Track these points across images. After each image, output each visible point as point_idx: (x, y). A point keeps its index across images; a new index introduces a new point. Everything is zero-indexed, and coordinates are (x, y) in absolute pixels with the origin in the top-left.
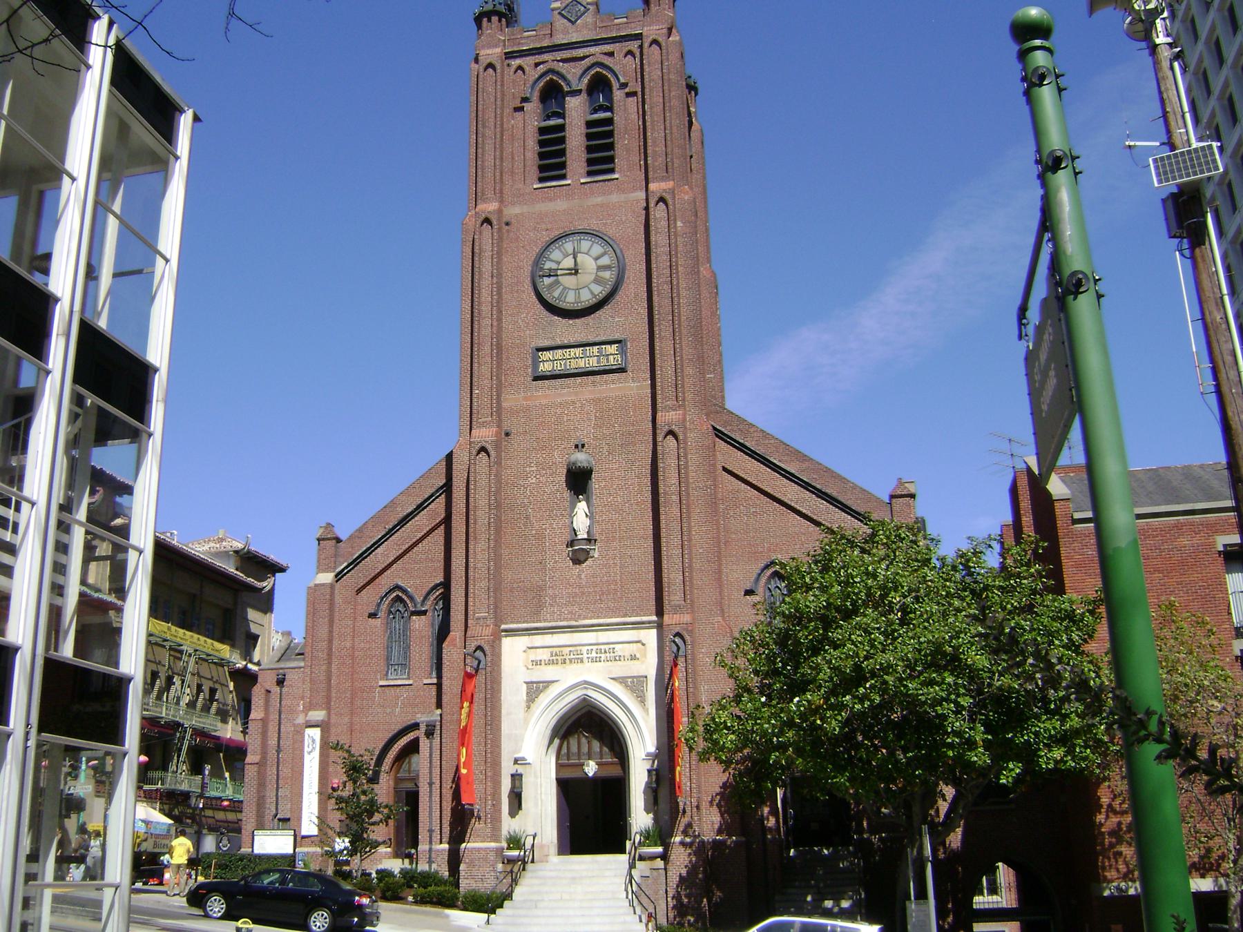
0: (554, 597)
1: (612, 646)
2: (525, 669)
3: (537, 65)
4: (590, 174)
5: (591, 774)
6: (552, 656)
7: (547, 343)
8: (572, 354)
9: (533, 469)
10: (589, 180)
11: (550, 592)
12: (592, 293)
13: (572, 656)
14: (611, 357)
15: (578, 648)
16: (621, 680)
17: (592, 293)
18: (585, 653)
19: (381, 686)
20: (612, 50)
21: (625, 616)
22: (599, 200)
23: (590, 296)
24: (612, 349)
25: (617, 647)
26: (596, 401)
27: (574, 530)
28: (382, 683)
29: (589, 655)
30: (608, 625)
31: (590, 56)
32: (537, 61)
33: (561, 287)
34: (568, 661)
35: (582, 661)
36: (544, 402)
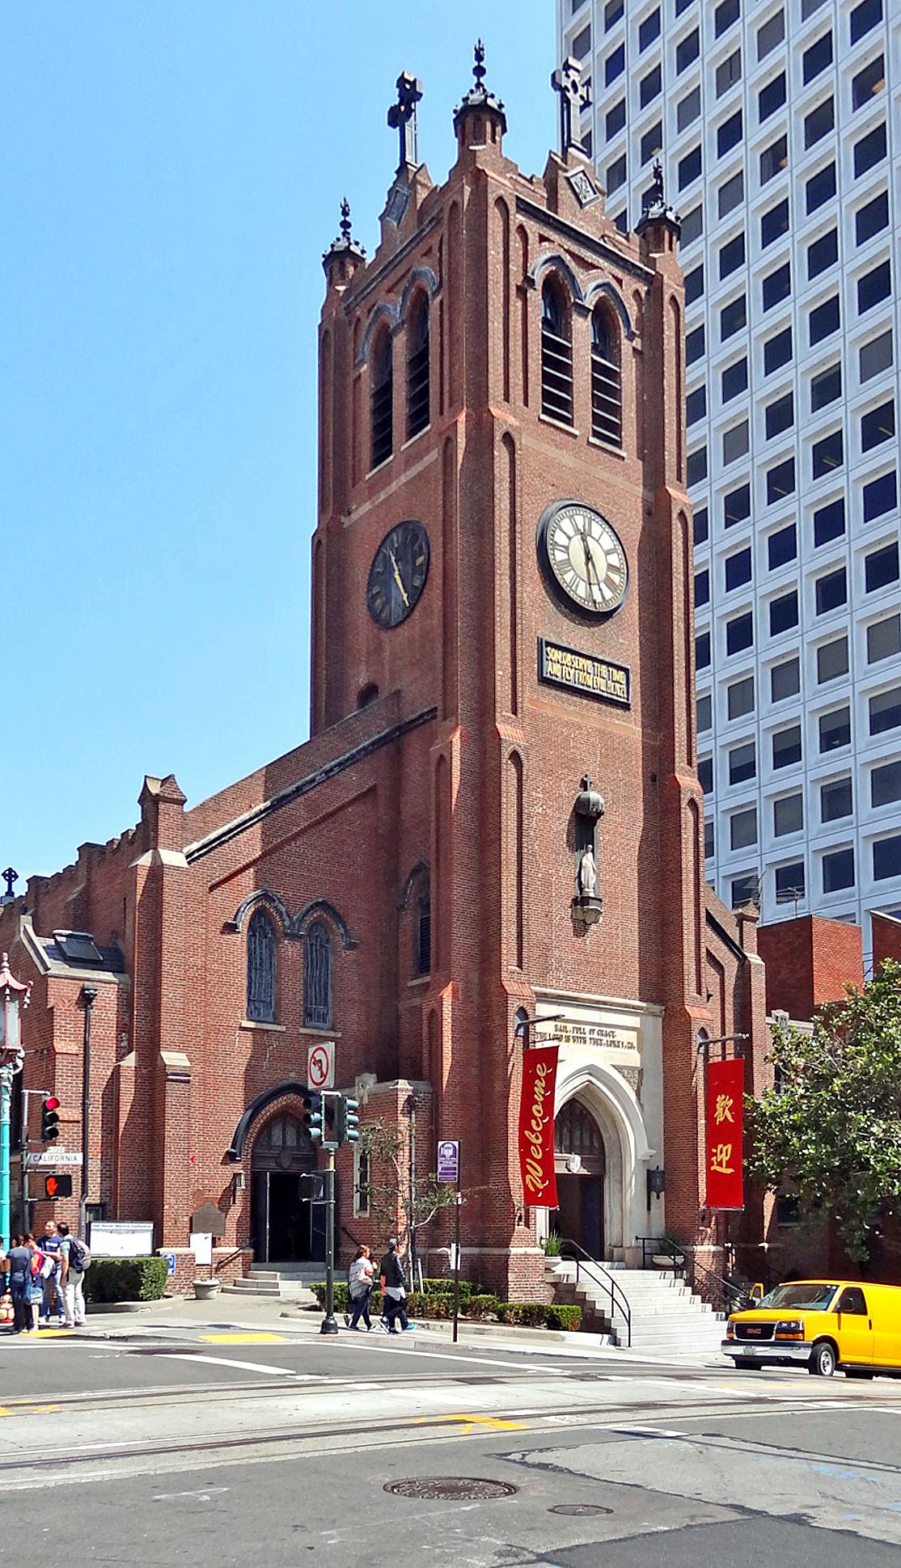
0: (560, 960)
1: (613, 1030)
4: (596, 434)
7: (553, 640)
11: (556, 952)
13: (575, 1034)
14: (618, 685)
15: (582, 1026)
18: (588, 1032)
20: (620, 274)
22: (605, 475)
24: (620, 676)
25: (618, 1032)
26: (602, 733)
27: (580, 883)
29: (591, 1036)
30: (612, 1004)
31: (598, 268)
33: (572, 572)
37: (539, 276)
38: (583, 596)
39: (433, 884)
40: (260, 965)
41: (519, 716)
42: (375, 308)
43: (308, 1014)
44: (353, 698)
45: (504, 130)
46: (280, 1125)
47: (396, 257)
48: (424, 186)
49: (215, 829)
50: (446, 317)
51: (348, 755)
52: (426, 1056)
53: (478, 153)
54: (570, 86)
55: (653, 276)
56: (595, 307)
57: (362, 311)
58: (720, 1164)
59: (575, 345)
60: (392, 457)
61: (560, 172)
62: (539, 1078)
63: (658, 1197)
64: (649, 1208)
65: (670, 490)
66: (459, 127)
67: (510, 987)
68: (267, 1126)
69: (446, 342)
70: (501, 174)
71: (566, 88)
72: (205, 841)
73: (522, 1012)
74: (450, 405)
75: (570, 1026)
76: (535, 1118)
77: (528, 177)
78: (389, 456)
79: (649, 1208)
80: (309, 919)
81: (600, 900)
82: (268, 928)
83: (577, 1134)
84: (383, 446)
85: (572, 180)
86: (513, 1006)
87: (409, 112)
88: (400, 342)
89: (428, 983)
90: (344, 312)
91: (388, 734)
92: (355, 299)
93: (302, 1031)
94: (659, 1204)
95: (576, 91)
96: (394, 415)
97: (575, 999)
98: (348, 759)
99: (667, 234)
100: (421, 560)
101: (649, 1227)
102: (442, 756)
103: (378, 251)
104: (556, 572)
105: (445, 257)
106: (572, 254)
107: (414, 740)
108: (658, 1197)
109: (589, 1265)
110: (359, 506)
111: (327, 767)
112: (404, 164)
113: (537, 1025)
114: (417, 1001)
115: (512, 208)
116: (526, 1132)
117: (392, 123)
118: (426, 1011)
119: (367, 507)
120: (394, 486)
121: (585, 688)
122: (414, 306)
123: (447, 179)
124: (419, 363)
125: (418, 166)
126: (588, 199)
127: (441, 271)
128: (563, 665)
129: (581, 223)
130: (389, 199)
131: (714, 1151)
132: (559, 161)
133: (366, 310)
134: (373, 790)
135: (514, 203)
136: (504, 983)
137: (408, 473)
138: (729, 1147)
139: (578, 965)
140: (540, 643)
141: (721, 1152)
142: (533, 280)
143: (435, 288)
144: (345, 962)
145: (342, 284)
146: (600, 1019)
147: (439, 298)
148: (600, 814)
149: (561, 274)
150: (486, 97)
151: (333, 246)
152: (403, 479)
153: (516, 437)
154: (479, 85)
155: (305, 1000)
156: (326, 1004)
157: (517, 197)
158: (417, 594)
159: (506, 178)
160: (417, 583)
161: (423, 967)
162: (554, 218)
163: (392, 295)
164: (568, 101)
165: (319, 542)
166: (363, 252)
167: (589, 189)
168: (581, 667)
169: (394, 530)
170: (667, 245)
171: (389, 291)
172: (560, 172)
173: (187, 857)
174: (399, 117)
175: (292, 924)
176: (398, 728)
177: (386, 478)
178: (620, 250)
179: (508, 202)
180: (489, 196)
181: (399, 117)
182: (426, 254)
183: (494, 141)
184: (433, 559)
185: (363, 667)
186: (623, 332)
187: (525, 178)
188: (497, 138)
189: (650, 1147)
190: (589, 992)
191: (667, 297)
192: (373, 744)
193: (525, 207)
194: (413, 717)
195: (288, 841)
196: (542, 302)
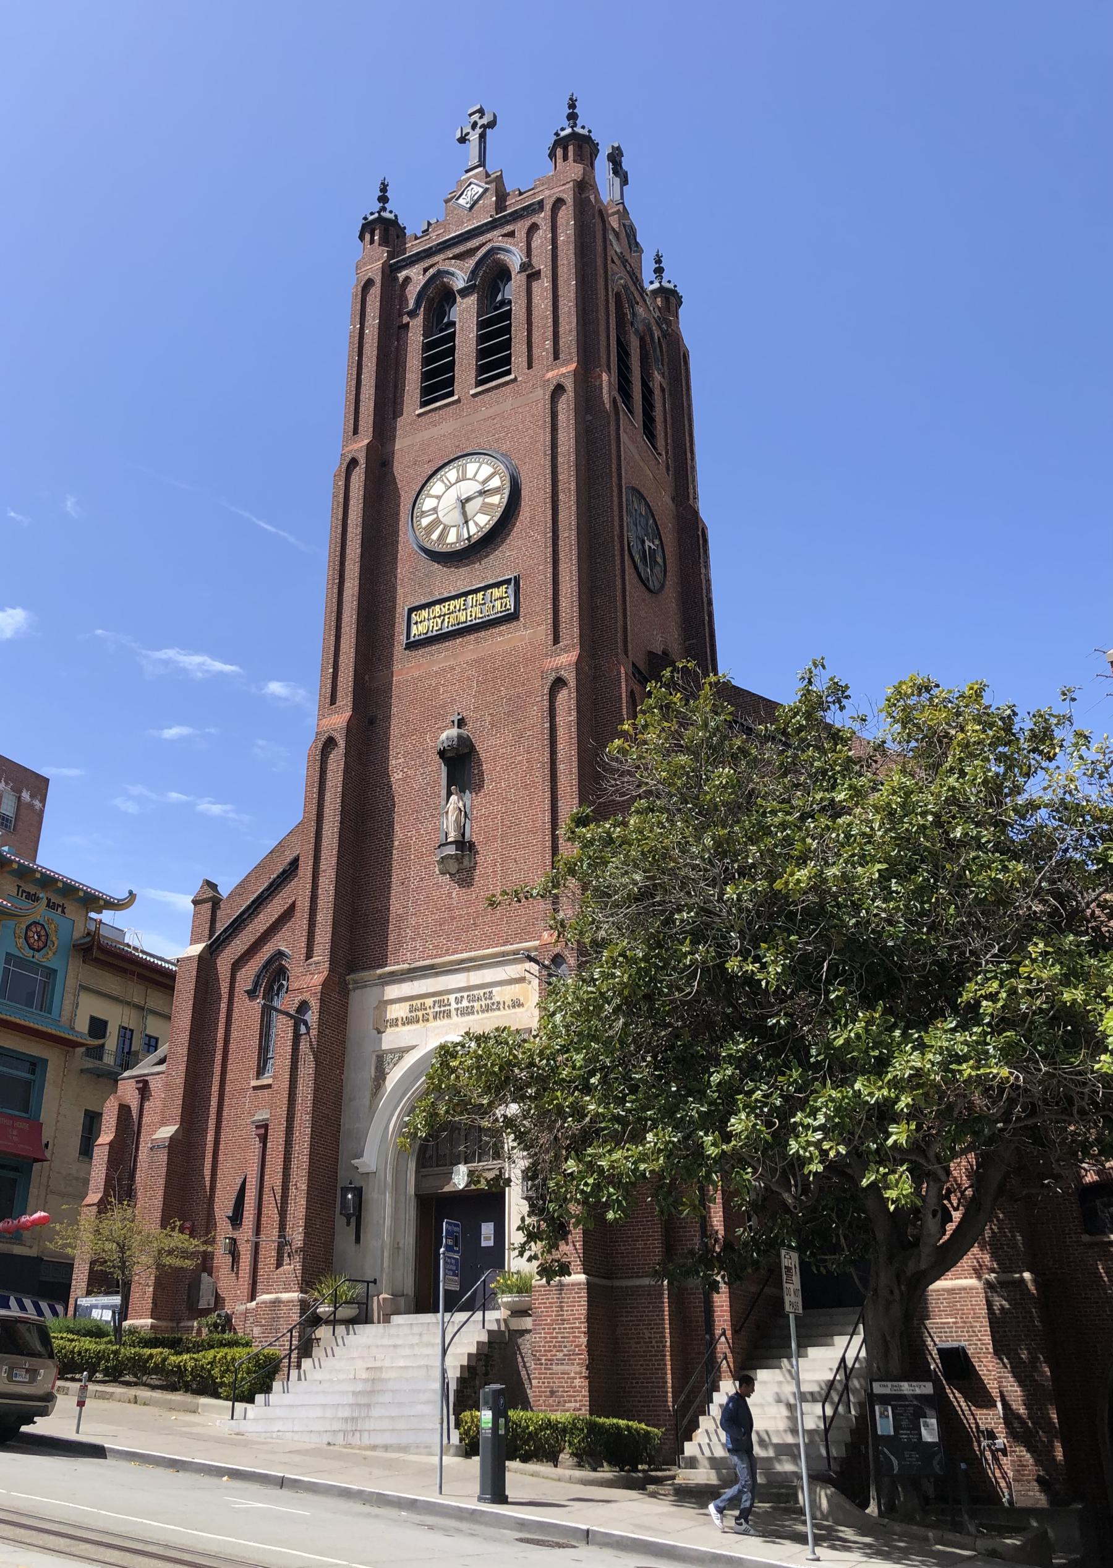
1: (487, 990)
2: (375, 1032)
3: (426, 270)
6: (411, 1011)
8: (452, 607)
9: (400, 761)
10: (480, 389)
13: (437, 1009)
15: (445, 997)
18: (452, 1000)
19: (255, 1088)
21: (505, 944)
25: (495, 990)
28: (254, 1083)
29: (460, 1005)
30: (483, 957)
32: (427, 265)
33: (442, 526)
34: (431, 1017)
35: (449, 1016)
36: (416, 674)
97: (432, 967)
139: (440, 925)
146: (468, 981)
190: (453, 953)
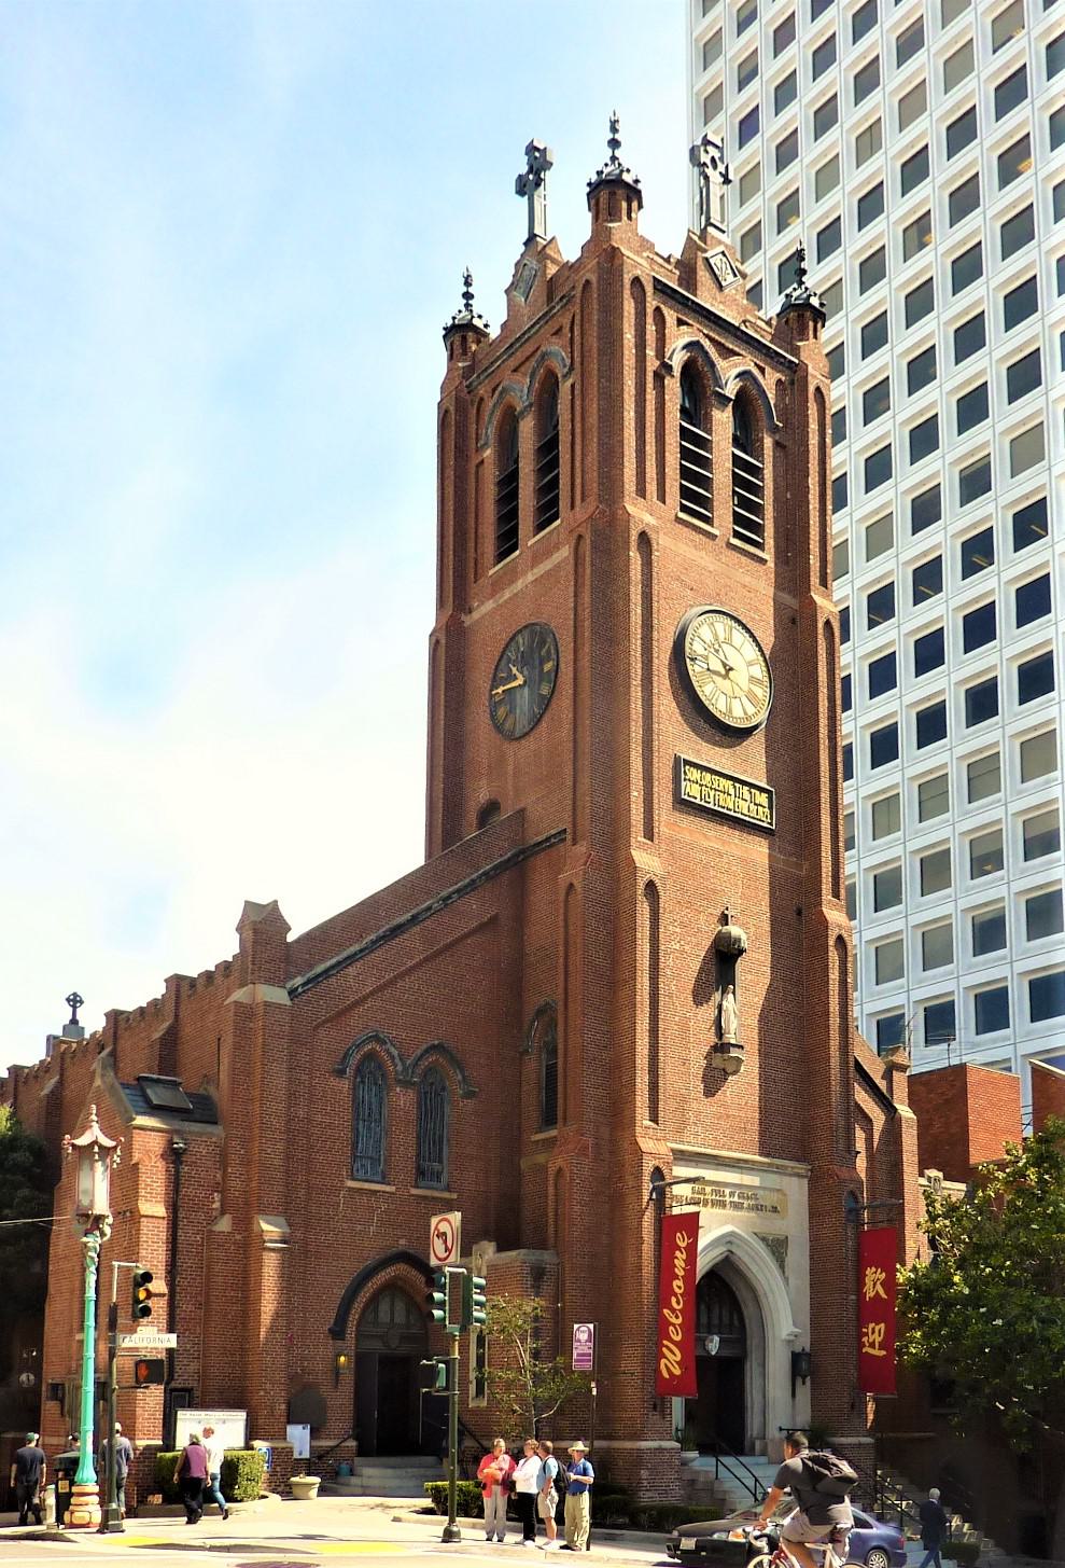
4: (737, 535)
5: (713, 1353)
11: (694, 1105)
12: (745, 713)
13: (714, 1197)
14: (760, 809)
16: (764, 1239)
17: (745, 713)
22: (747, 579)
23: (742, 715)
37: (677, 361)
38: (724, 710)
39: (561, 1028)
40: (364, 1114)
41: (656, 841)
42: (500, 388)
43: (421, 1173)
44: (472, 817)
45: (640, 206)
46: (387, 1299)
47: (524, 334)
48: (554, 261)
49: (322, 960)
50: (578, 403)
51: (467, 881)
52: (551, 1221)
53: (613, 231)
54: (709, 163)
55: (797, 365)
56: (736, 396)
57: (486, 391)
58: (872, 1345)
59: (715, 438)
60: (517, 552)
61: (699, 253)
62: (679, 1248)
63: (804, 1383)
64: (794, 1395)
65: (816, 597)
66: (593, 202)
67: (646, 1144)
68: (374, 1299)
69: (578, 430)
70: (638, 253)
71: (705, 164)
72: (311, 974)
73: (658, 1173)
74: (583, 500)
75: (708, 1189)
76: (676, 1295)
77: (666, 257)
78: (514, 551)
79: (794, 1395)
80: (424, 1064)
81: (742, 1047)
82: (378, 1074)
83: (716, 1311)
84: (508, 541)
85: (711, 260)
86: (648, 1167)
87: (538, 183)
88: (527, 427)
89: (555, 1137)
90: (466, 390)
91: (513, 856)
92: (478, 377)
93: (414, 1191)
94: (804, 1392)
95: (715, 167)
96: (520, 506)
97: (715, 1157)
98: (466, 887)
99: (811, 324)
100: (548, 666)
101: (793, 1417)
102: (571, 885)
103: (504, 326)
104: (695, 684)
105: (577, 338)
106: (712, 340)
107: (540, 862)
108: (804, 1383)
109: (728, 1460)
110: (483, 603)
111: (444, 893)
112: (531, 239)
113: (673, 1187)
114: (541, 1159)
115: (649, 289)
116: (666, 1311)
117: (521, 191)
118: (552, 1171)
119: (489, 605)
120: (519, 585)
121: (725, 811)
122: (542, 384)
123: (579, 255)
124: (548, 449)
125: (549, 238)
126: (727, 283)
127: (572, 352)
128: (701, 785)
129: (721, 307)
130: (517, 272)
131: (865, 1330)
132: (696, 238)
133: (490, 390)
134: (494, 920)
135: (651, 285)
136: (639, 1139)
137: (535, 571)
138: (882, 1325)
140: (677, 759)
141: (873, 1332)
142: (671, 366)
143: (566, 370)
144: (460, 1111)
145: (464, 361)
147: (571, 381)
148: (741, 951)
149: (700, 360)
150: (622, 171)
151: (454, 318)
152: (530, 577)
153: (653, 536)
154: (614, 159)
155: (418, 1155)
156: (441, 1162)
157: (654, 278)
158: (546, 703)
159: (642, 257)
160: (545, 691)
161: (549, 1119)
162: (693, 302)
163: (518, 376)
164: (707, 178)
165: (437, 642)
166: (486, 326)
167: (730, 271)
168: (721, 788)
169: (520, 631)
170: (811, 333)
171: (515, 371)
172: (699, 253)
173: (289, 993)
174: (529, 183)
175: (405, 1069)
176: (522, 852)
177: (511, 575)
178: (762, 336)
179: (645, 283)
180: (625, 276)
181: (529, 183)
182: (556, 333)
183: (630, 218)
184: (562, 666)
185: (484, 782)
186: (764, 423)
187: (662, 258)
188: (633, 215)
189: (795, 1325)
190: (730, 1149)
191: (811, 389)
192: (495, 868)
193: (661, 288)
194: (540, 839)
195: (402, 976)
196: (679, 390)
